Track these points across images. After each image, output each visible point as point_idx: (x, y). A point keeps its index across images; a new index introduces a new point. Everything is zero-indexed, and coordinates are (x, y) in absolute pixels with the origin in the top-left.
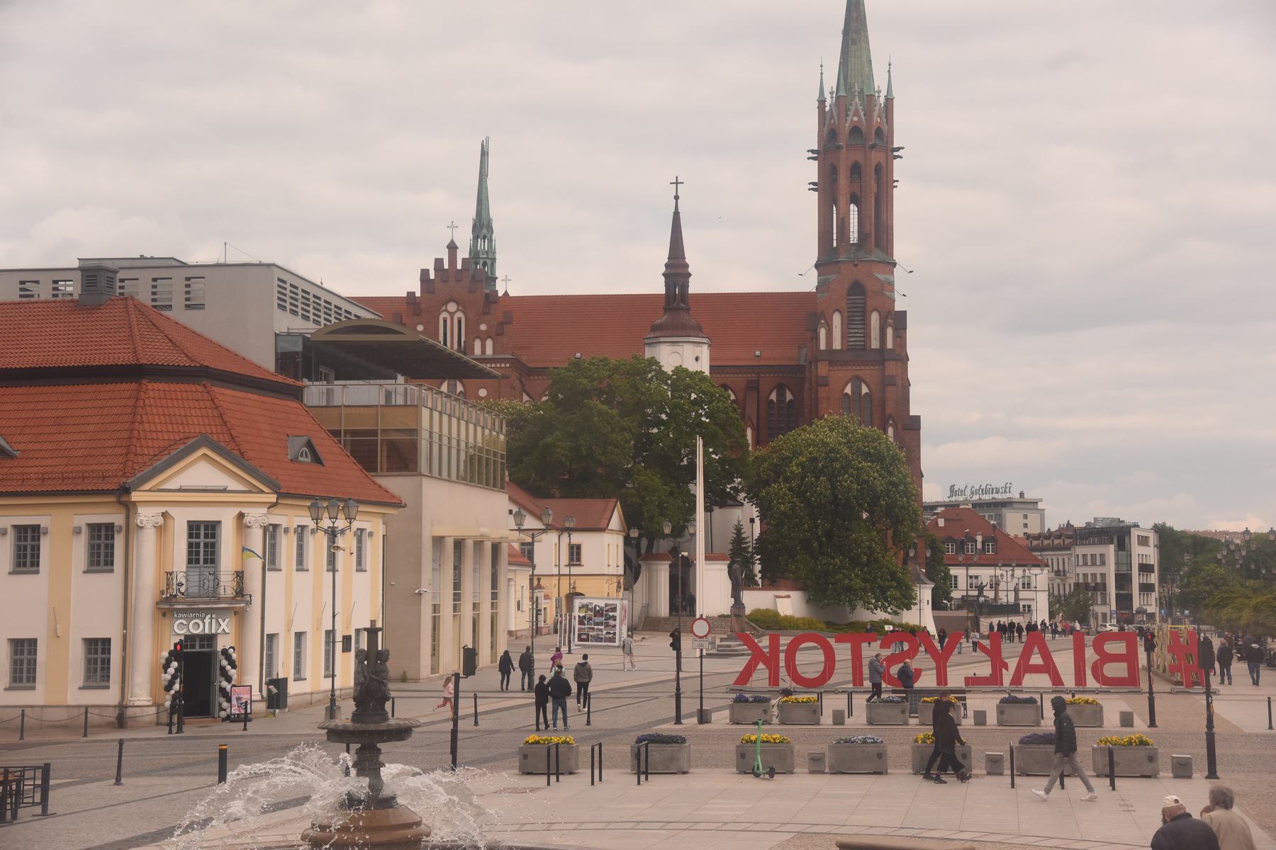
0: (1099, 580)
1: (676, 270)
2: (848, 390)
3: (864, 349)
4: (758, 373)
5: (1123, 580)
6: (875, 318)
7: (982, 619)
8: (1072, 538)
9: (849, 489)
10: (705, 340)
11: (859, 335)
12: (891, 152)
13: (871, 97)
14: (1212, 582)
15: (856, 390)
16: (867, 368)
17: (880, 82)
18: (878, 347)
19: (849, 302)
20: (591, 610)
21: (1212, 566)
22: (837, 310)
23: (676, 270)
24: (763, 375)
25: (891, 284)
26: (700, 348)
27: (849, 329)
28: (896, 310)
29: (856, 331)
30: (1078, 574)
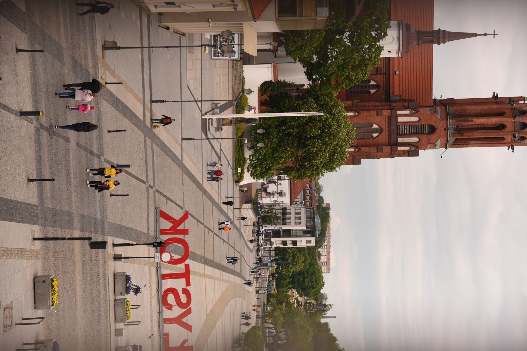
0: (287, 221)
2: (375, 126)
3: (398, 134)
4: (385, 74)
5: (288, 233)
6: (415, 139)
7: (250, 205)
8: (310, 206)
9: (313, 147)
10: (400, 56)
11: (406, 131)
12: (511, 146)
14: (294, 259)
15: (375, 131)
16: (387, 136)
18: (399, 142)
19: (424, 125)
20: (231, 42)
21: (303, 259)
24: (384, 76)
25: (434, 147)
26: (396, 53)
27: (409, 125)
28: (420, 151)
29: (408, 130)
30: (291, 209)
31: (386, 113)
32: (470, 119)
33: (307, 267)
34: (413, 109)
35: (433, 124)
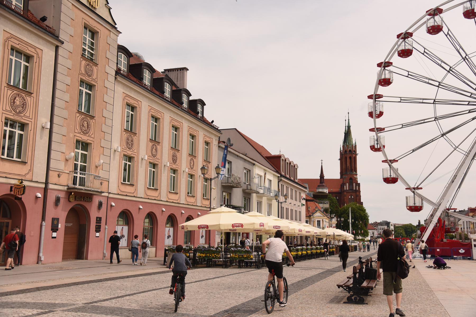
1: (322, 175)
2: (350, 197)
6: (354, 184)
9: (358, 216)
12: (356, 155)
13: (353, 145)
15: (351, 197)
17: (354, 142)
22: (347, 183)
23: (322, 175)
25: (357, 178)
31: (345, 193)
32: (347, 167)
33: (403, 229)
34: (344, 185)
35: (349, 178)
